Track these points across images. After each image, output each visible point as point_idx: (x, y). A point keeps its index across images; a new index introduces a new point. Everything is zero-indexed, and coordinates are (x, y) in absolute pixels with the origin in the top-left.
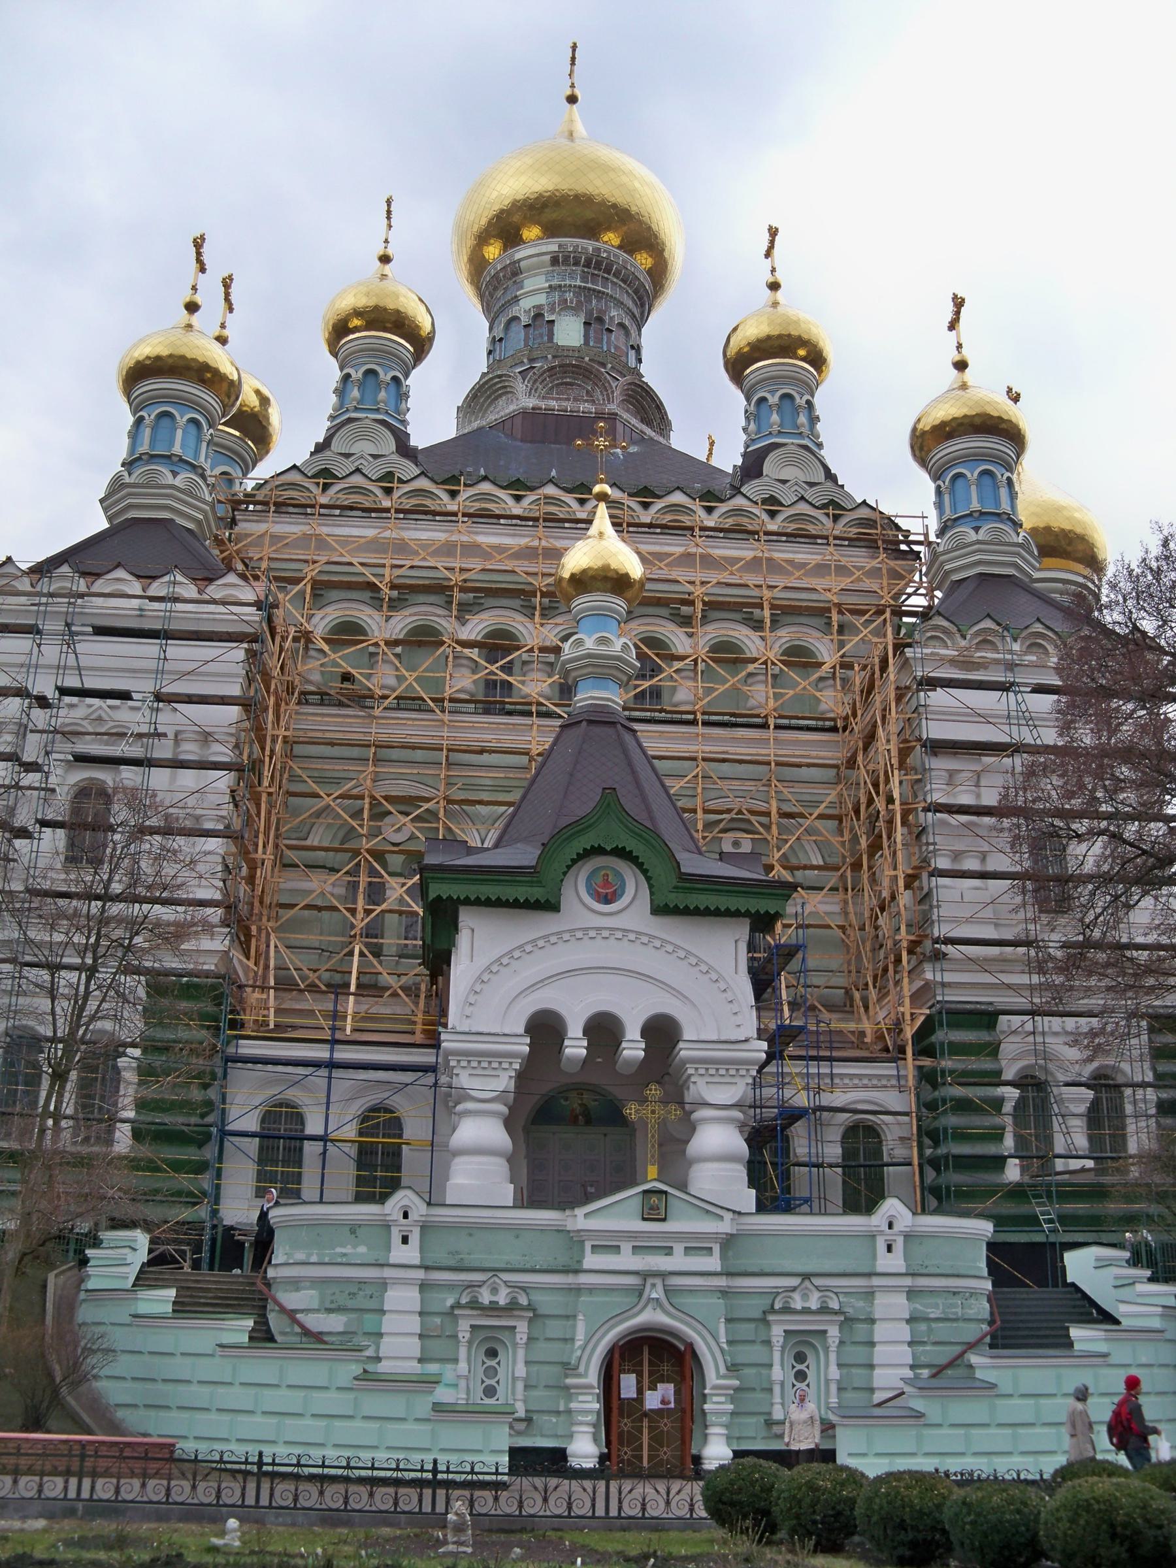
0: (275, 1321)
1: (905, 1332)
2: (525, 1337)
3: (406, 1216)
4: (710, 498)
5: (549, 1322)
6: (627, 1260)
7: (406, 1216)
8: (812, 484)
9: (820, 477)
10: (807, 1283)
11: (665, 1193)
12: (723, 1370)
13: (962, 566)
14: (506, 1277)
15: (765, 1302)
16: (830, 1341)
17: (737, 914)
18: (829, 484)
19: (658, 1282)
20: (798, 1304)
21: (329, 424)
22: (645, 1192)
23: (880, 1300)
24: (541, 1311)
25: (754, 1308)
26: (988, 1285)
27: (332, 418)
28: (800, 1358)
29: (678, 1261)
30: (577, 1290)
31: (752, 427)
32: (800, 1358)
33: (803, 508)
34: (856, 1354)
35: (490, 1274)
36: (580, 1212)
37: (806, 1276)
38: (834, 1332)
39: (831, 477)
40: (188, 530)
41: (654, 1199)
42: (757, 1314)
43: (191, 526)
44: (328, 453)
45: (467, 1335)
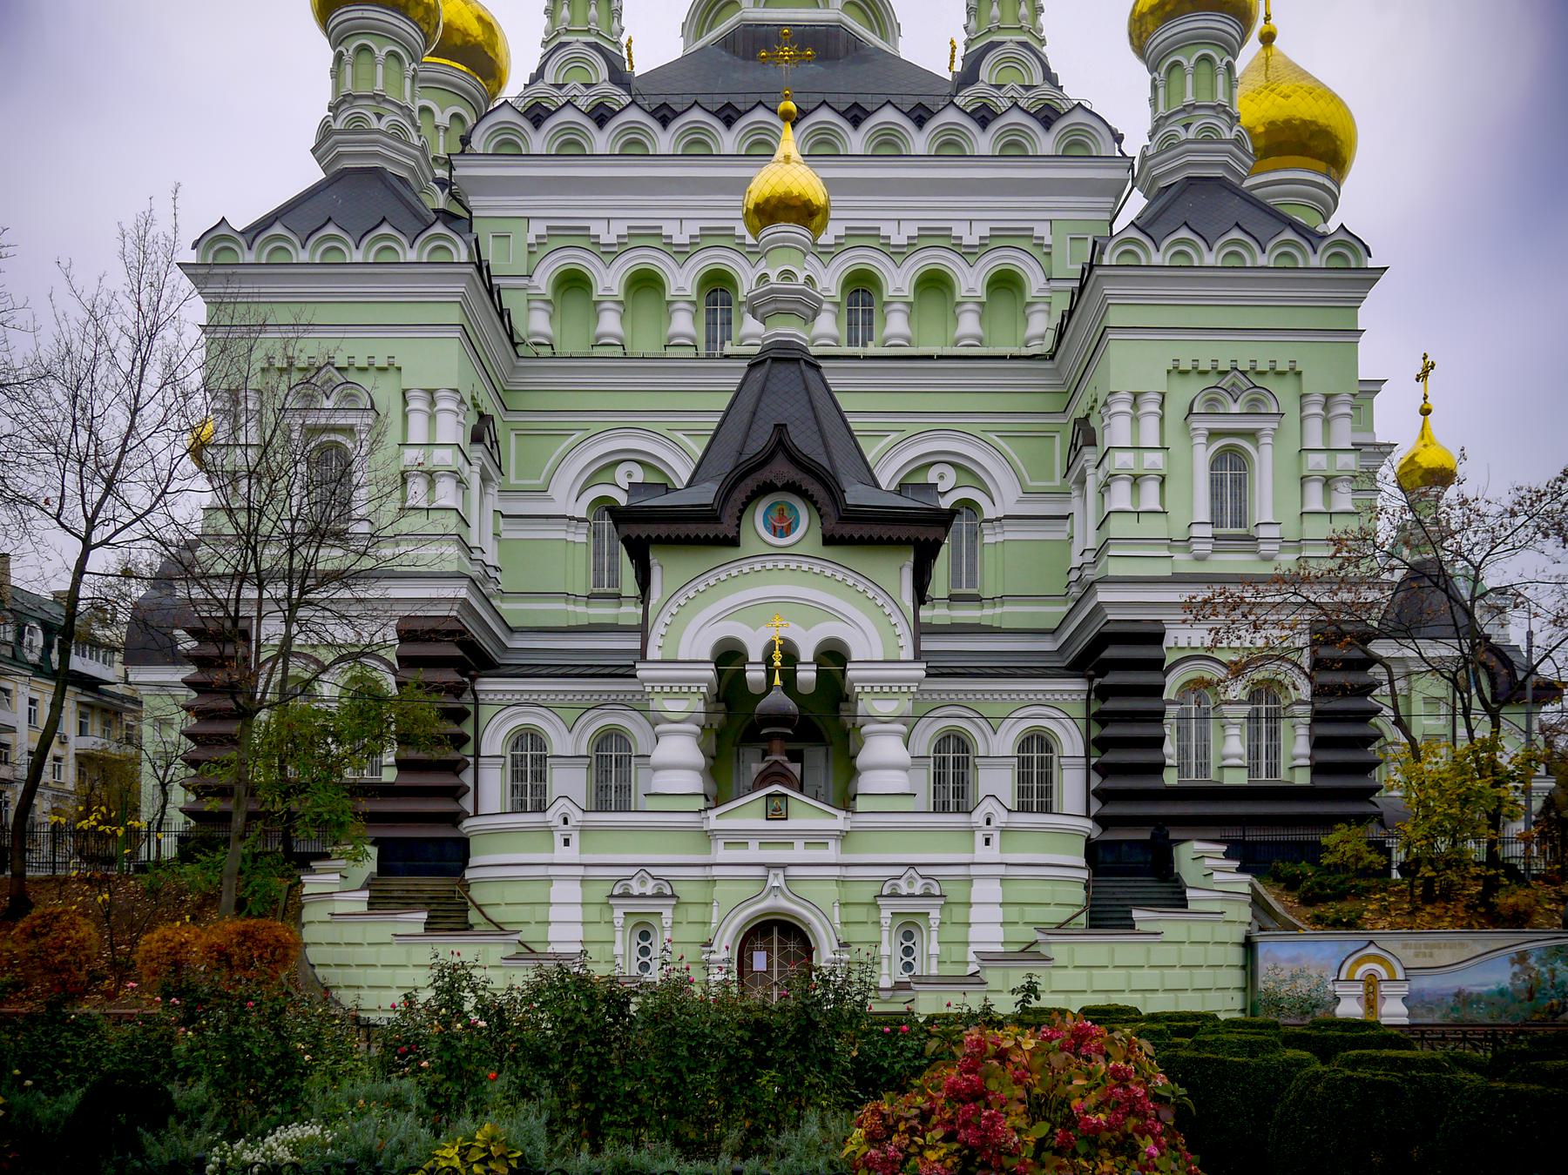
0: (473, 916)
1: (998, 914)
2: (670, 921)
3: (566, 821)
4: (920, 117)
5: (691, 908)
6: (754, 853)
7: (566, 821)
8: (1028, 88)
9: (1038, 78)
10: (912, 872)
11: (786, 795)
12: (836, 947)
13: (1172, 171)
14: (654, 871)
15: (875, 889)
16: (931, 922)
17: (908, 542)
18: (1047, 86)
19: (780, 872)
20: (904, 890)
21: (543, 51)
22: (768, 796)
23: (978, 886)
24: (683, 899)
25: (866, 893)
26: (1085, 874)
27: (545, 43)
28: (908, 936)
29: (799, 853)
30: (712, 881)
31: (973, 24)
32: (908, 936)
33: (1016, 117)
34: (954, 933)
35: (639, 869)
36: (712, 814)
37: (912, 866)
38: (935, 914)
39: (1050, 78)
40: (400, 178)
41: (777, 802)
42: (869, 899)
43: (404, 174)
44: (540, 85)
45: (622, 921)
